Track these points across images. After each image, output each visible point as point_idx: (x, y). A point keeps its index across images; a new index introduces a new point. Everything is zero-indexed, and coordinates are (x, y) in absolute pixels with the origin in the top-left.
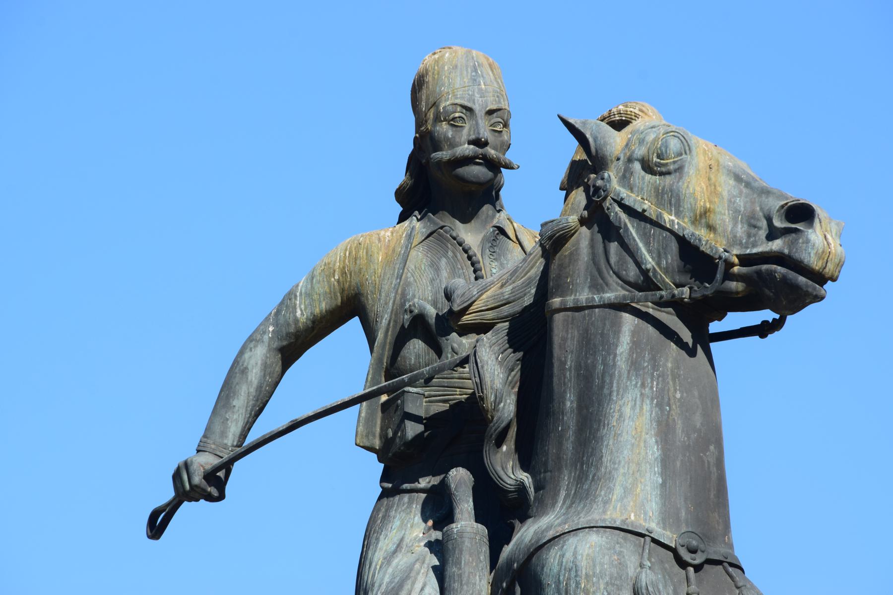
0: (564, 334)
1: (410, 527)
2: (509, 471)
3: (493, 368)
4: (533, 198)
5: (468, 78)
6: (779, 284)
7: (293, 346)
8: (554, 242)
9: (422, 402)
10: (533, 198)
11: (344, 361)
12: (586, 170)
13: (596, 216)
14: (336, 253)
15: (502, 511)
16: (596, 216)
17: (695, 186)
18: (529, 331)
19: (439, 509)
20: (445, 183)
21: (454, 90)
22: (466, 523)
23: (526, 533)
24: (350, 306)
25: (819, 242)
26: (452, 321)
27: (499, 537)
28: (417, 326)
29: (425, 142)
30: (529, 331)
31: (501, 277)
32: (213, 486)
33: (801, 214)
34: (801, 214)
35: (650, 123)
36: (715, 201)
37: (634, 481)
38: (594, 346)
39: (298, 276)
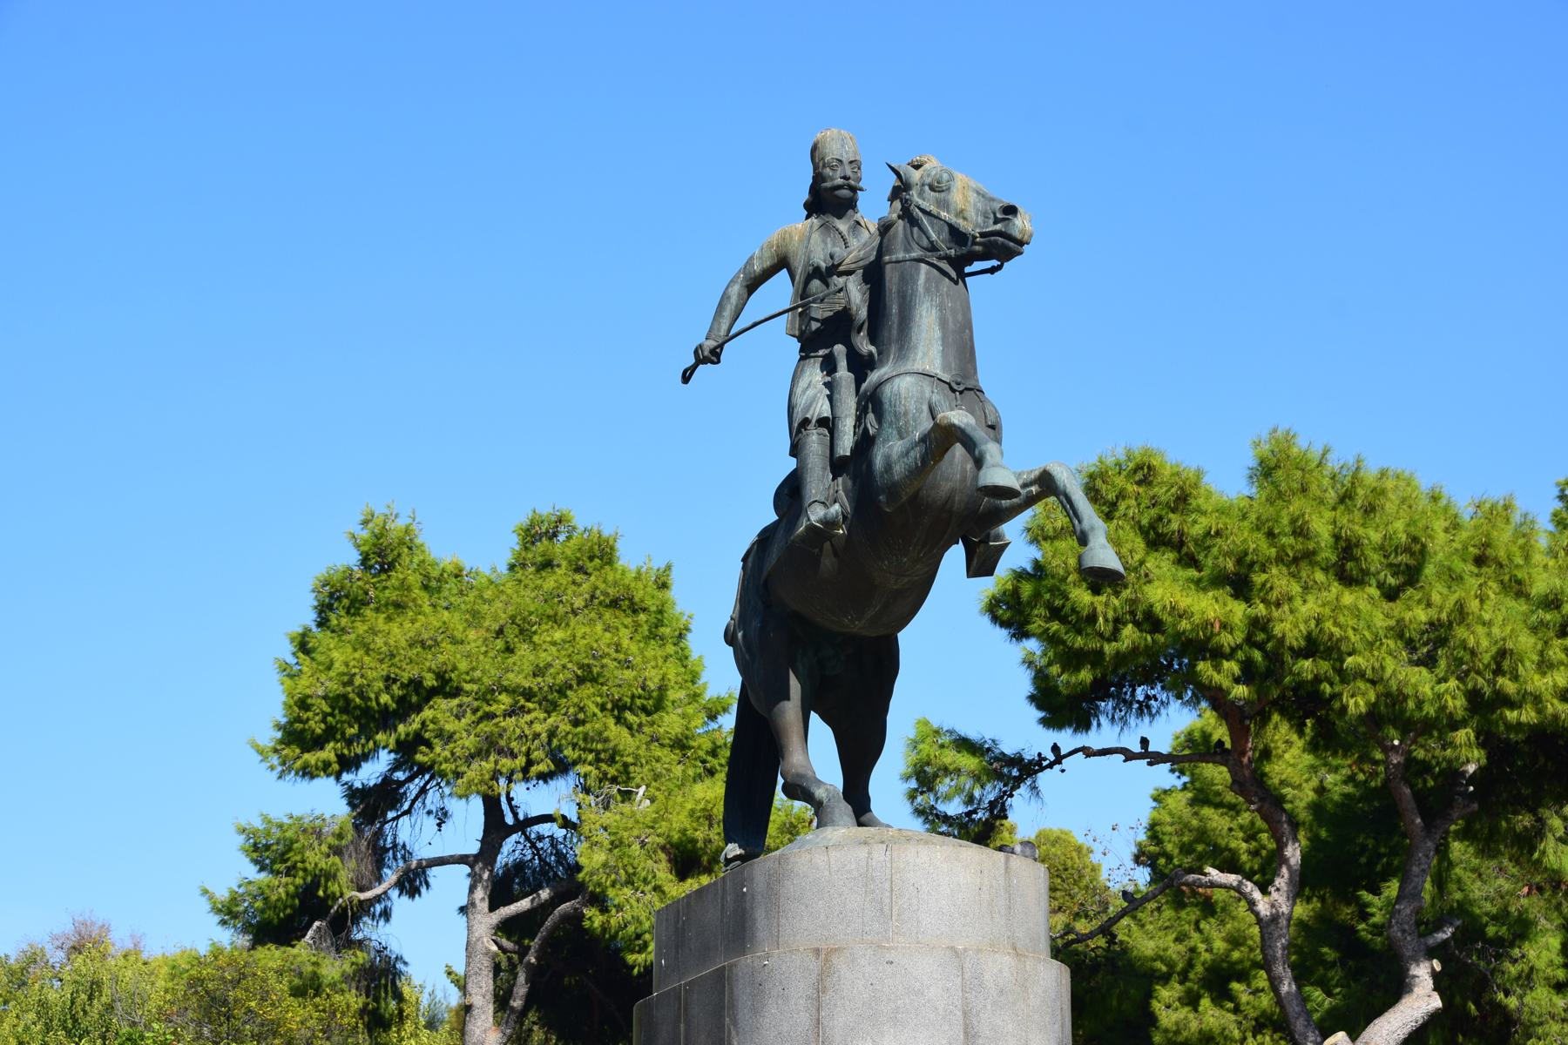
0: (891, 276)
1: (815, 375)
2: (865, 346)
3: (855, 293)
4: (874, 206)
5: (839, 146)
6: (999, 246)
7: (754, 284)
8: (885, 228)
9: (820, 311)
10: (874, 206)
11: (779, 291)
12: (900, 191)
13: (906, 214)
14: (774, 236)
15: (861, 366)
16: (906, 214)
17: (956, 198)
18: (874, 274)
19: (829, 366)
20: (829, 199)
21: (833, 151)
22: (843, 373)
23: (874, 377)
24: (782, 263)
25: (1020, 224)
26: (834, 270)
27: (860, 380)
28: (816, 273)
29: (818, 178)
30: (874, 274)
31: (859, 248)
32: (714, 356)
33: (1011, 210)
34: (1011, 210)
35: (933, 165)
36: (966, 204)
37: (928, 349)
38: (907, 281)
39: (753, 248)
